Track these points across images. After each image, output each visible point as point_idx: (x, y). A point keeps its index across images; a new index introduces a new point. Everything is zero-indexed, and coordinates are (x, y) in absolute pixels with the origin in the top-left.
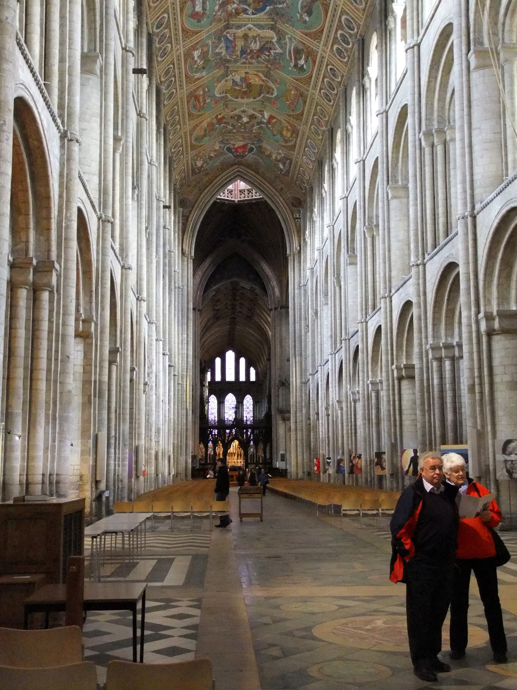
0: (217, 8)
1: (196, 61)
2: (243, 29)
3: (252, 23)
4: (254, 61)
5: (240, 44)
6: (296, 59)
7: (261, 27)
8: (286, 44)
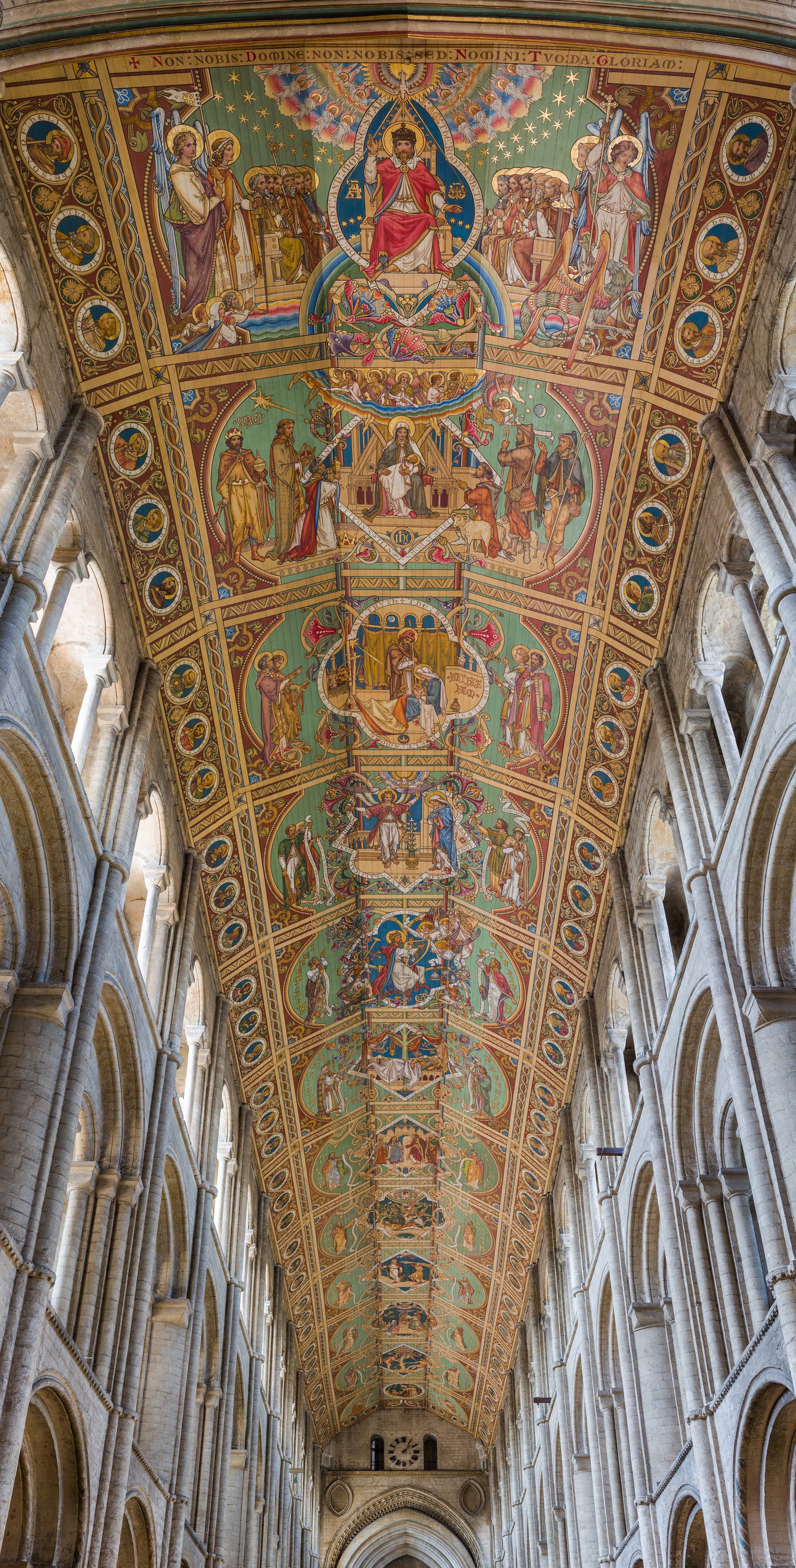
0: (465, 952)
3: (400, 897)
4: (390, 785)
5: (423, 840)
6: (304, 860)
7: (384, 886)
8: (331, 875)
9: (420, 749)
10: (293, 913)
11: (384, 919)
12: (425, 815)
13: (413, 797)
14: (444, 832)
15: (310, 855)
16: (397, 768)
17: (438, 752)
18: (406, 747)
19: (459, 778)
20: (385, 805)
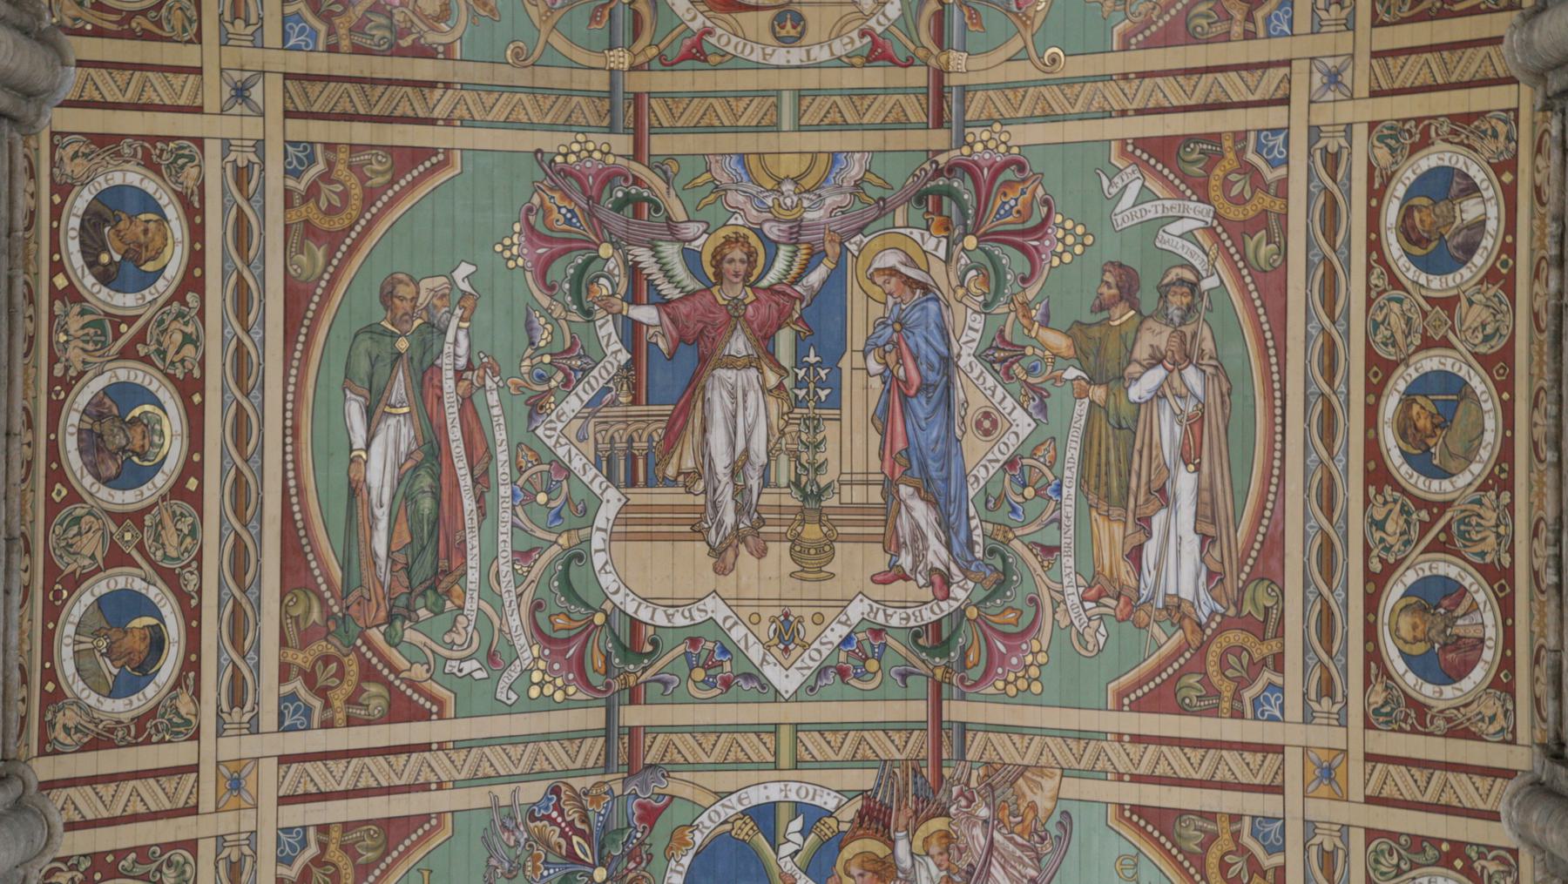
1: (1189, 455)
2: (837, 633)
3: (769, 713)
4: (742, 211)
8: (524, 556)
9: (840, 63)
10: (368, 674)
11: (708, 824)
12: (857, 338)
13: (815, 256)
14: (921, 406)
15: (455, 434)
16: (766, 142)
17: (896, 76)
18: (796, 56)
19: (967, 168)
20: (722, 295)
